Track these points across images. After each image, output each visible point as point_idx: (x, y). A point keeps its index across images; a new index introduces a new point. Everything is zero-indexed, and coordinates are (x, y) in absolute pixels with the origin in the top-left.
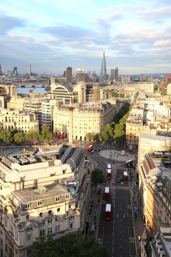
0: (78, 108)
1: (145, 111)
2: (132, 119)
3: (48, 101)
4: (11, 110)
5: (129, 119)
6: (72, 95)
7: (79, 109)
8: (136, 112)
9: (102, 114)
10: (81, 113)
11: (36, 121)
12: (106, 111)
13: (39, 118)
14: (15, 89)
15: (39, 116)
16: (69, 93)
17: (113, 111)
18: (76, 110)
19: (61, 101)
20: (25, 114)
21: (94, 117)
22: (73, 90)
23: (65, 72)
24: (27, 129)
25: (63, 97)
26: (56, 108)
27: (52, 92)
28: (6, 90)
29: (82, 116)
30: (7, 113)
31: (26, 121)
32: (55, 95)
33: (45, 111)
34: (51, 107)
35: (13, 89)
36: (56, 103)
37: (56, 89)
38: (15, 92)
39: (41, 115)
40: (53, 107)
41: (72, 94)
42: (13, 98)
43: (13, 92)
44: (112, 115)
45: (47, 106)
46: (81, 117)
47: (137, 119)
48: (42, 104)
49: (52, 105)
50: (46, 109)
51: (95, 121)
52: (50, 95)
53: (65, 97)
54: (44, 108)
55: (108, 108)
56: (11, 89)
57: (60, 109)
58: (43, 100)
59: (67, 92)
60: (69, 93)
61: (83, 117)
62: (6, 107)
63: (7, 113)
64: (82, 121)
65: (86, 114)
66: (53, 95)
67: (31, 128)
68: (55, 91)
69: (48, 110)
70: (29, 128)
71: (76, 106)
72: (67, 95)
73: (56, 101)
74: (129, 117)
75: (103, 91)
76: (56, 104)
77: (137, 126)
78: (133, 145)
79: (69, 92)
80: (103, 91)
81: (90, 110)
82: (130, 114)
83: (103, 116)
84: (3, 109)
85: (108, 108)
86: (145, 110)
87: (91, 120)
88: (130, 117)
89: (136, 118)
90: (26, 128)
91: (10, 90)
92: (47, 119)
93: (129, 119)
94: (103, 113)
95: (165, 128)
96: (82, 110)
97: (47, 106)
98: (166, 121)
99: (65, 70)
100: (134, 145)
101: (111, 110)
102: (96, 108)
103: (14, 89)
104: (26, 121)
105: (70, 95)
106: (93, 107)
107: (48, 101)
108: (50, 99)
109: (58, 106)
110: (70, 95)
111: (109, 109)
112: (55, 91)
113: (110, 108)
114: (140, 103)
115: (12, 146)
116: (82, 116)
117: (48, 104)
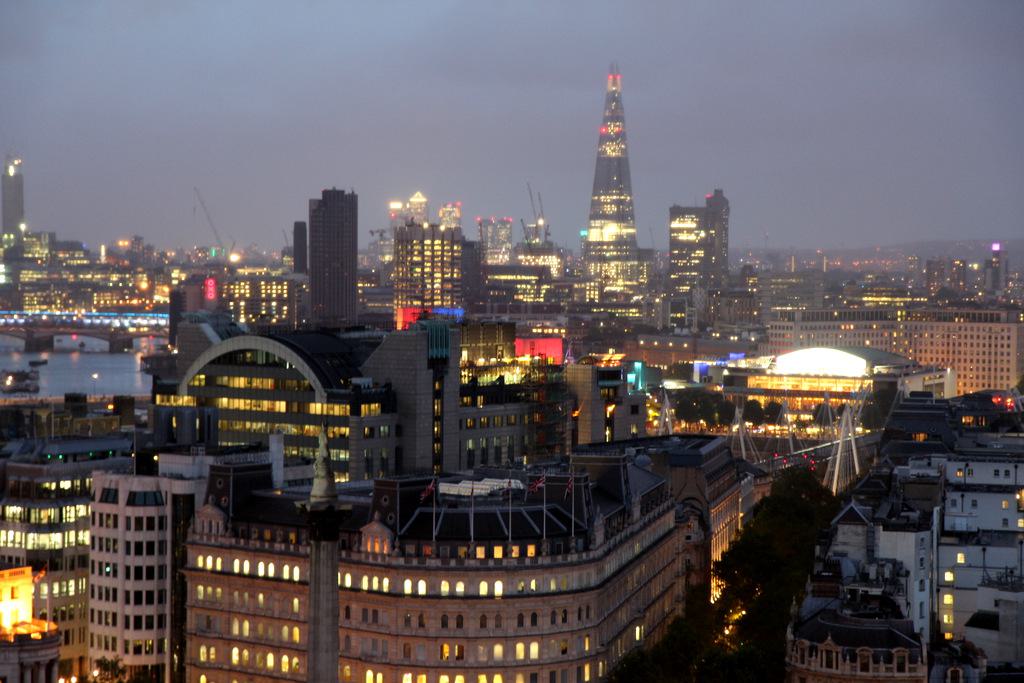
0: (395, 517)
1: (945, 540)
2: (834, 604)
3: (147, 468)
5: (811, 603)
7: (402, 526)
8: (870, 550)
9: (594, 560)
10: (415, 562)
12: (622, 542)
17: (678, 541)
19: (251, 457)
22: (360, 375)
23: (299, 228)
26: (208, 517)
33: (121, 546)
34: (168, 510)
36: (206, 472)
44: (667, 576)
45: (133, 499)
50: (128, 528)
55: (637, 513)
57: (242, 527)
58: (103, 455)
65: (453, 563)
69: (144, 536)
71: (376, 505)
73: (210, 460)
74: (809, 587)
76: (211, 489)
77: (882, 666)
79: (326, 383)
81: (490, 533)
82: (818, 567)
85: (637, 513)
86: (943, 533)
88: (817, 593)
89: (866, 597)
92: (131, 610)
93: (811, 603)
94: (592, 555)
97: (133, 499)
99: (305, 217)
106: (510, 508)
111: (650, 522)
113: (655, 519)
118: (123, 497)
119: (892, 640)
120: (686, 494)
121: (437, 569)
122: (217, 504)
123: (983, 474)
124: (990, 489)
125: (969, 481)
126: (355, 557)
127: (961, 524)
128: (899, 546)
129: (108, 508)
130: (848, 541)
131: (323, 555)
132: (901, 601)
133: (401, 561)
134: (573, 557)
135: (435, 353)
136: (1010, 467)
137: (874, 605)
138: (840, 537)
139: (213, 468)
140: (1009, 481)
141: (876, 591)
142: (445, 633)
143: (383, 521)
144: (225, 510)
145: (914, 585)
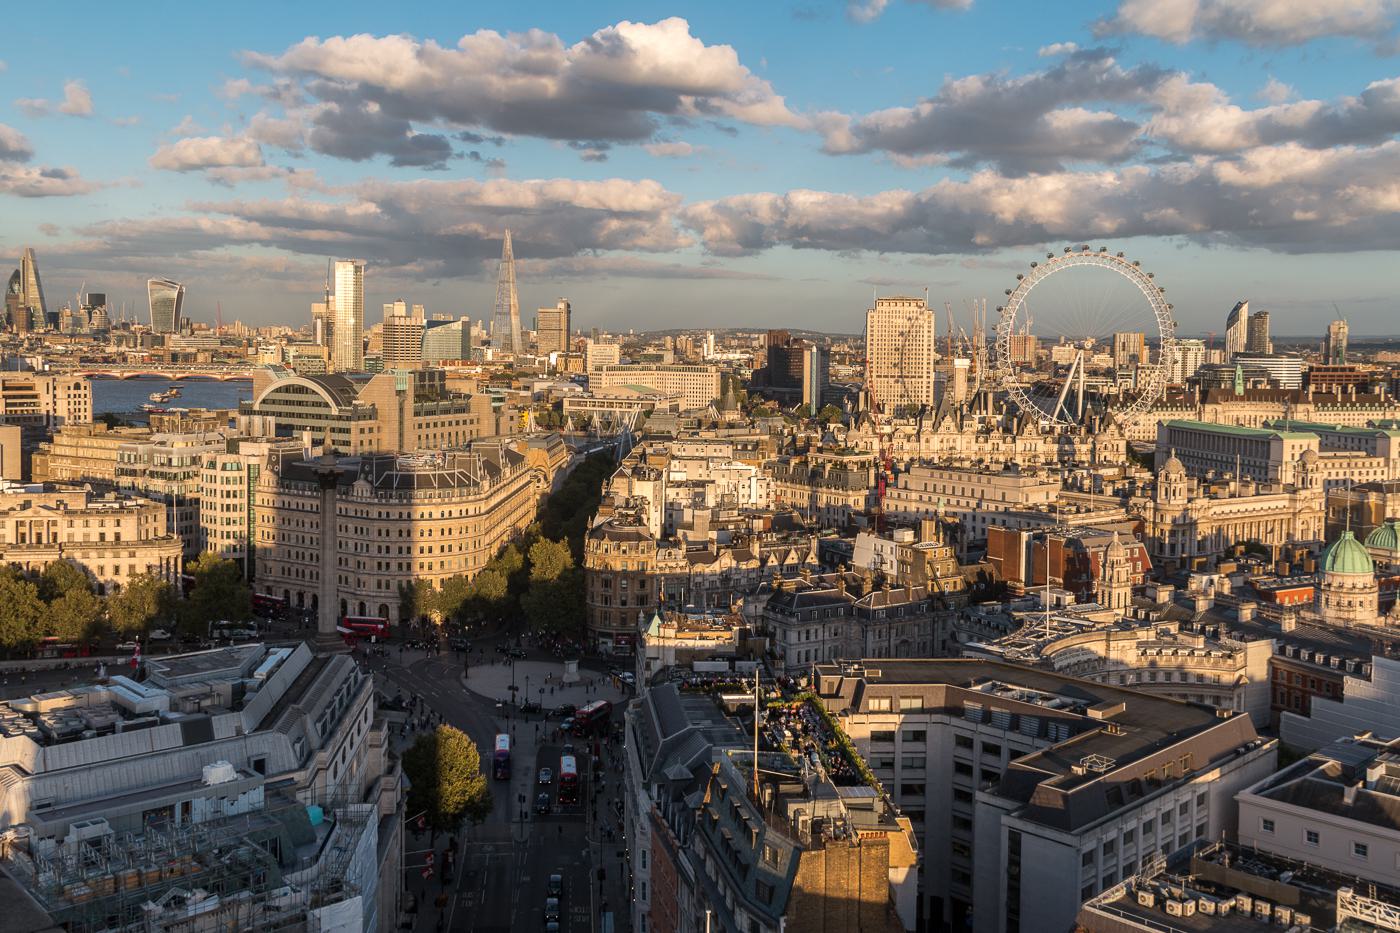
4: (49, 488)
6: (348, 419)
8: (630, 491)
11: (168, 539)
13: (185, 524)
14: (82, 392)
15: (183, 517)
16: (335, 411)
17: (532, 488)
18: (361, 488)
20: (116, 506)
21: (443, 515)
24: (124, 580)
25: (304, 428)
27: (256, 407)
28: (35, 397)
29: (388, 514)
30: (26, 506)
31: (118, 536)
32: (269, 418)
34: (244, 474)
35: (72, 392)
36: (266, 452)
37: (278, 390)
38: (82, 407)
39: (198, 509)
40: (253, 477)
41: (349, 414)
42: (68, 436)
43: (72, 407)
46: (384, 516)
47: (630, 519)
48: (205, 461)
49: (249, 466)
51: (446, 532)
52: (244, 420)
53: (313, 429)
54: (213, 479)
55: (507, 471)
56: (60, 393)
59: (327, 405)
60: (335, 411)
61: (392, 517)
62: (26, 476)
63: (26, 506)
64: (388, 535)
66: (257, 420)
67: (141, 569)
68: (274, 402)
70: (132, 567)
71: (363, 470)
72: (280, 414)
73: (269, 445)
75: (495, 400)
76: (270, 461)
78: (618, 635)
79: (338, 404)
80: (495, 400)
83: (482, 511)
84: (8, 485)
85: (508, 474)
87: (450, 530)
88: (603, 514)
90: (117, 570)
91: (55, 396)
93: (599, 520)
94: (483, 496)
95: (755, 558)
96: (387, 484)
98: (758, 525)
100: (624, 635)
101: (521, 483)
102: (452, 476)
103: (77, 392)
104: (118, 536)
105: (339, 418)
107: (232, 447)
108: (244, 436)
109: (279, 468)
110: (339, 418)
112: (274, 402)
114: (649, 451)
115: (43, 658)
116: (388, 514)
117: (230, 458)
118: (219, 466)
119: (639, 537)
120: (537, 463)
121: (396, 505)
122: (272, 470)
123: (691, 450)
124: (692, 458)
125: (684, 454)
126: (350, 499)
127: (676, 477)
128: (644, 489)
129: (212, 472)
130: (619, 488)
131: (327, 497)
132: (644, 516)
133: (376, 501)
134: (470, 498)
135: (399, 388)
136: (703, 447)
137: (630, 519)
138: (615, 485)
139: (270, 450)
140: (702, 454)
141: (632, 512)
142: (401, 539)
143: (366, 479)
144: (277, 473)
145: (652, 509)
